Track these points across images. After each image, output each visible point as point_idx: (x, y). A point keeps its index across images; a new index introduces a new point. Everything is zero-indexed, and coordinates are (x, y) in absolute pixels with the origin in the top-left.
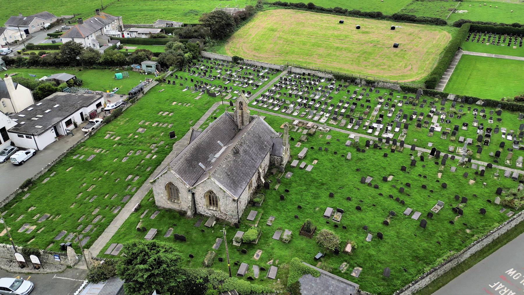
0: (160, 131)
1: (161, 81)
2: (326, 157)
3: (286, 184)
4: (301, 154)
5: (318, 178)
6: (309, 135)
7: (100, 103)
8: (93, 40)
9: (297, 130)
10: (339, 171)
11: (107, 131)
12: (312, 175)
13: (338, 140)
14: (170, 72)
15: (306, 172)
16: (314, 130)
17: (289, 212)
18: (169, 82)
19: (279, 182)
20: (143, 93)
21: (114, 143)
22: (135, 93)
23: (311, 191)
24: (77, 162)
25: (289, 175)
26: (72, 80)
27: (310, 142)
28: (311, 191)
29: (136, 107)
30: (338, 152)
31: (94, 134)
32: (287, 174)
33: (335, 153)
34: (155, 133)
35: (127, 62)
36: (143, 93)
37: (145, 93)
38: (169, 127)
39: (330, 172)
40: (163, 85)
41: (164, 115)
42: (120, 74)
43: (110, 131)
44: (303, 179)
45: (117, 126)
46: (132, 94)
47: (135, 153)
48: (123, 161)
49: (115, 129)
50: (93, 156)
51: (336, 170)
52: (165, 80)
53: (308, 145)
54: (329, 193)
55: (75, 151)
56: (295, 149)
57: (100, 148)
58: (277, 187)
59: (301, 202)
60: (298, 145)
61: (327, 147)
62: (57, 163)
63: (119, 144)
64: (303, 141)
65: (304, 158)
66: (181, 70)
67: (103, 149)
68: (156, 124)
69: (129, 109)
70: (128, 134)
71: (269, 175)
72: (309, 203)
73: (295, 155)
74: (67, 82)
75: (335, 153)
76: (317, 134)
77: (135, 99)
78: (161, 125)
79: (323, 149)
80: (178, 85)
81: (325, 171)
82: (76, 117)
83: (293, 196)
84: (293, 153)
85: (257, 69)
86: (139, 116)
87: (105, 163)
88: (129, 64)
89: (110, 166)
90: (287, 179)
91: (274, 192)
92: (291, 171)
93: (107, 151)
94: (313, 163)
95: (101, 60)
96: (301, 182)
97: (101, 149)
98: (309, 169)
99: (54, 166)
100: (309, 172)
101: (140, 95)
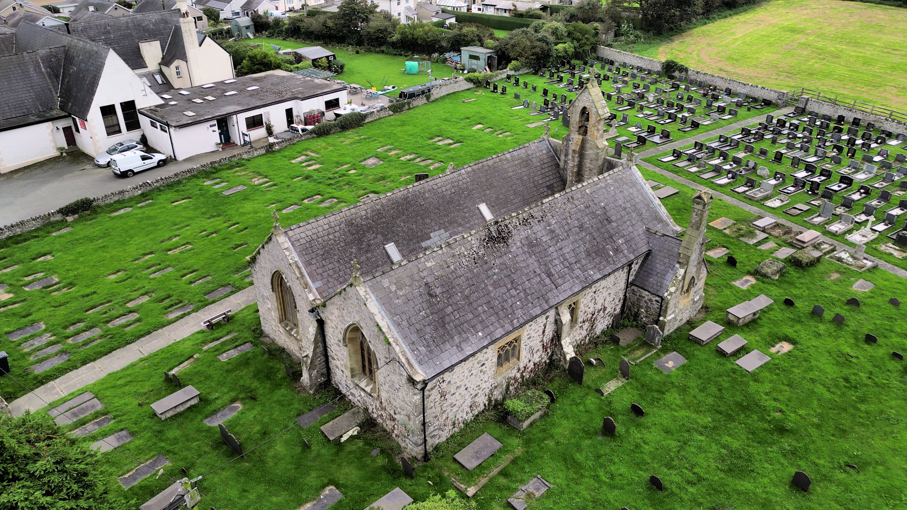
0: (406, 171)
1: (478, 83)
2: (830, 343)
3: (645, 388)
4: (741, 311)
5: (770, 404)
6: (795, 262)
7: (337, 100)
8: (409, 9)
9: (760, 243)
10: (863, 400)
11: (307, 149)
12: (753, 387)
13: (894, 302)
14: (508, 71)
15: (734, 371)
16: (816, 254)
17: (612, 487)
18: (495, 88)
19: (625, 372)
20: (428, 98)
21: (299, 173)
22: (412, 95)
23: (726, 439)
24: (203, 192)
25: (671, 362)
26: (324, 60)
27: (792, 284)
28: (726, 439)
29: (396, 120)
30: (880, 340)
31: (279, 151)
32: (664, 358)
33: (870, 339)
34: (392, 172)
35: (442, 47)
36: (428, 98)
37: (432, 98)
38: (431, 168)
39: (827, 395)
40: (481, 92)
41: (440, 143)
42: (416, 63)
43: (312, 151)
44: (713, 389)
45: (334, 145)
46: (405, 96)
47: (322, 201)
48: (284, 211)
49: (325, 148)
50: (240, 188)
51: (853, 395)
52: (488, 83)
53: (775, 291)
54: (793, 471)
55: (217, 171)
56: (727, 292)
57: (266, 177)
58: (611, 387)
59: (669, 466)
60: (745, 283)
61: (843, 313)
62: (168, 185)
63: (307, 178)
64: (765, 276)
65: (747, 325)
66: (536, 73)
67: (271, 180)
68: (412, 157)
69: (383, 120)
70: (339, 164)
71: (604, 343)
72: (700, 479)
73: (721, 309)
74: (314, 60)
75: (870, 339)
76: (820, 268)
77: (403, 105)
78: (418, 160)
79: (828, 315)
80: (509, 97)
81: (807, 385)
82: (275, 116)
83: (650, 436)
84: (714, 301)
85: (711, 92)
86: (388, 136)
87: (248, 206)
88: (442, 50)
89: (251, 215)
90: (658, 371)
91: (591, 401)
92: (682, 352)
93: (275, 185)
94: (773, 350)
95: (396, 37)
96: (701, 396)
97: (266, 180)
98: (751, 362)
99: (158, 189)
100: (744, 373)
101: (421, 101)
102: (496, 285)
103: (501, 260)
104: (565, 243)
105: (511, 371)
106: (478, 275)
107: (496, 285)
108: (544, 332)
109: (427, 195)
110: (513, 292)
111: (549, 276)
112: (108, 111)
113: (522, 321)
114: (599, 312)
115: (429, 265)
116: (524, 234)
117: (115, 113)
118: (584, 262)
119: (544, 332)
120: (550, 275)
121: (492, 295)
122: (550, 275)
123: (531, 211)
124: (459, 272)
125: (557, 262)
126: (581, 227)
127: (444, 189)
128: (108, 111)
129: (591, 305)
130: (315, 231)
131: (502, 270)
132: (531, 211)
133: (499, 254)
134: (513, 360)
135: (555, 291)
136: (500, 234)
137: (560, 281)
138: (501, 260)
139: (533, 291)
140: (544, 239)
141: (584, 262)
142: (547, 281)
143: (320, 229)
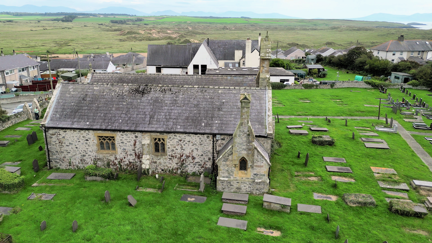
102: (117, 109)
103: (132, 101)
104: (178, 108)
105: (107, 155)
106: (112, 101)
107: (117, 109)
108: (135, 145)
109: (166, 80)
110: (123, 116)
111: (150, 118)
112: (196, 67)
113: (113, 128)
114: (188, 157)
115: (95, 88)
116: (157, 95)
117: (198, 68)
118: (180, 120)
119: (135, 145)
120: (152, 117)
121: (111, 112)
122: (152, 117)
123: (172, 88)
124: (106, 97)
125: (163, 114)
126: (197, 106)
127: (177, 81)
128: (196, 67)
129: (179, 147)
130: (105, 77)
131: (128, 104)
132: (172, 88)
133: (134, 98)
134: (111, 152)
135: (147, 125)
136: (144, 90)
137: (154, 123)
138: (132, 101)
139: (134, 119)
140: (166, 102)
141: (180, 120)
142: (147, 119)
143: (107, 77)
